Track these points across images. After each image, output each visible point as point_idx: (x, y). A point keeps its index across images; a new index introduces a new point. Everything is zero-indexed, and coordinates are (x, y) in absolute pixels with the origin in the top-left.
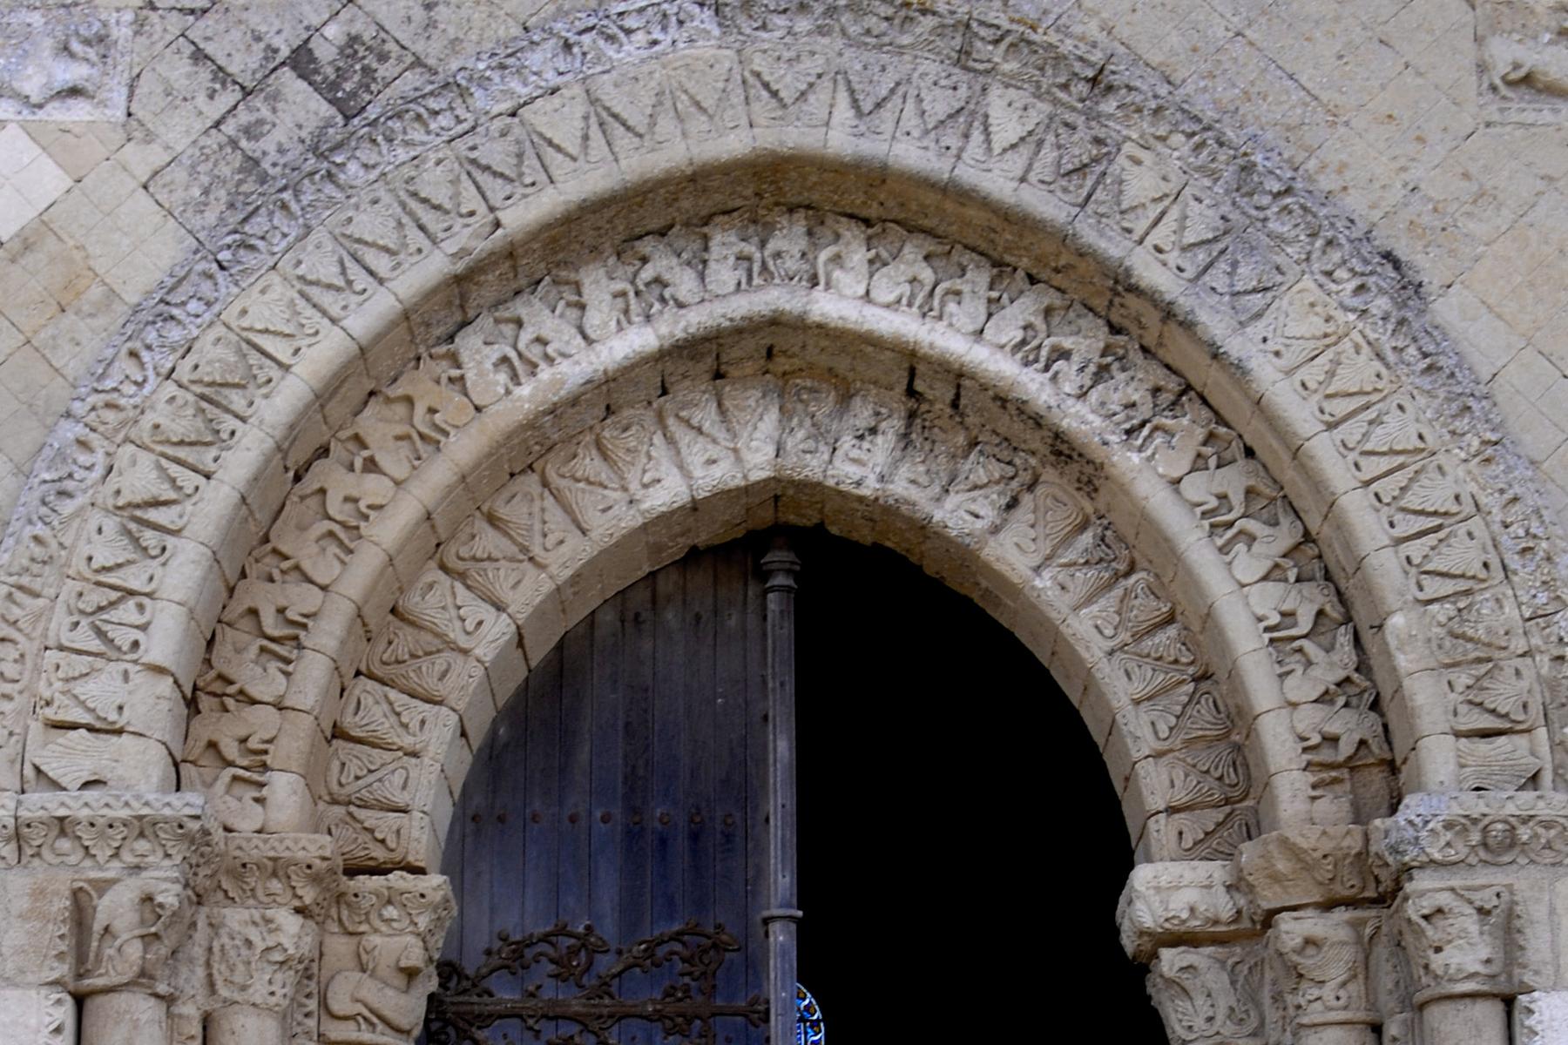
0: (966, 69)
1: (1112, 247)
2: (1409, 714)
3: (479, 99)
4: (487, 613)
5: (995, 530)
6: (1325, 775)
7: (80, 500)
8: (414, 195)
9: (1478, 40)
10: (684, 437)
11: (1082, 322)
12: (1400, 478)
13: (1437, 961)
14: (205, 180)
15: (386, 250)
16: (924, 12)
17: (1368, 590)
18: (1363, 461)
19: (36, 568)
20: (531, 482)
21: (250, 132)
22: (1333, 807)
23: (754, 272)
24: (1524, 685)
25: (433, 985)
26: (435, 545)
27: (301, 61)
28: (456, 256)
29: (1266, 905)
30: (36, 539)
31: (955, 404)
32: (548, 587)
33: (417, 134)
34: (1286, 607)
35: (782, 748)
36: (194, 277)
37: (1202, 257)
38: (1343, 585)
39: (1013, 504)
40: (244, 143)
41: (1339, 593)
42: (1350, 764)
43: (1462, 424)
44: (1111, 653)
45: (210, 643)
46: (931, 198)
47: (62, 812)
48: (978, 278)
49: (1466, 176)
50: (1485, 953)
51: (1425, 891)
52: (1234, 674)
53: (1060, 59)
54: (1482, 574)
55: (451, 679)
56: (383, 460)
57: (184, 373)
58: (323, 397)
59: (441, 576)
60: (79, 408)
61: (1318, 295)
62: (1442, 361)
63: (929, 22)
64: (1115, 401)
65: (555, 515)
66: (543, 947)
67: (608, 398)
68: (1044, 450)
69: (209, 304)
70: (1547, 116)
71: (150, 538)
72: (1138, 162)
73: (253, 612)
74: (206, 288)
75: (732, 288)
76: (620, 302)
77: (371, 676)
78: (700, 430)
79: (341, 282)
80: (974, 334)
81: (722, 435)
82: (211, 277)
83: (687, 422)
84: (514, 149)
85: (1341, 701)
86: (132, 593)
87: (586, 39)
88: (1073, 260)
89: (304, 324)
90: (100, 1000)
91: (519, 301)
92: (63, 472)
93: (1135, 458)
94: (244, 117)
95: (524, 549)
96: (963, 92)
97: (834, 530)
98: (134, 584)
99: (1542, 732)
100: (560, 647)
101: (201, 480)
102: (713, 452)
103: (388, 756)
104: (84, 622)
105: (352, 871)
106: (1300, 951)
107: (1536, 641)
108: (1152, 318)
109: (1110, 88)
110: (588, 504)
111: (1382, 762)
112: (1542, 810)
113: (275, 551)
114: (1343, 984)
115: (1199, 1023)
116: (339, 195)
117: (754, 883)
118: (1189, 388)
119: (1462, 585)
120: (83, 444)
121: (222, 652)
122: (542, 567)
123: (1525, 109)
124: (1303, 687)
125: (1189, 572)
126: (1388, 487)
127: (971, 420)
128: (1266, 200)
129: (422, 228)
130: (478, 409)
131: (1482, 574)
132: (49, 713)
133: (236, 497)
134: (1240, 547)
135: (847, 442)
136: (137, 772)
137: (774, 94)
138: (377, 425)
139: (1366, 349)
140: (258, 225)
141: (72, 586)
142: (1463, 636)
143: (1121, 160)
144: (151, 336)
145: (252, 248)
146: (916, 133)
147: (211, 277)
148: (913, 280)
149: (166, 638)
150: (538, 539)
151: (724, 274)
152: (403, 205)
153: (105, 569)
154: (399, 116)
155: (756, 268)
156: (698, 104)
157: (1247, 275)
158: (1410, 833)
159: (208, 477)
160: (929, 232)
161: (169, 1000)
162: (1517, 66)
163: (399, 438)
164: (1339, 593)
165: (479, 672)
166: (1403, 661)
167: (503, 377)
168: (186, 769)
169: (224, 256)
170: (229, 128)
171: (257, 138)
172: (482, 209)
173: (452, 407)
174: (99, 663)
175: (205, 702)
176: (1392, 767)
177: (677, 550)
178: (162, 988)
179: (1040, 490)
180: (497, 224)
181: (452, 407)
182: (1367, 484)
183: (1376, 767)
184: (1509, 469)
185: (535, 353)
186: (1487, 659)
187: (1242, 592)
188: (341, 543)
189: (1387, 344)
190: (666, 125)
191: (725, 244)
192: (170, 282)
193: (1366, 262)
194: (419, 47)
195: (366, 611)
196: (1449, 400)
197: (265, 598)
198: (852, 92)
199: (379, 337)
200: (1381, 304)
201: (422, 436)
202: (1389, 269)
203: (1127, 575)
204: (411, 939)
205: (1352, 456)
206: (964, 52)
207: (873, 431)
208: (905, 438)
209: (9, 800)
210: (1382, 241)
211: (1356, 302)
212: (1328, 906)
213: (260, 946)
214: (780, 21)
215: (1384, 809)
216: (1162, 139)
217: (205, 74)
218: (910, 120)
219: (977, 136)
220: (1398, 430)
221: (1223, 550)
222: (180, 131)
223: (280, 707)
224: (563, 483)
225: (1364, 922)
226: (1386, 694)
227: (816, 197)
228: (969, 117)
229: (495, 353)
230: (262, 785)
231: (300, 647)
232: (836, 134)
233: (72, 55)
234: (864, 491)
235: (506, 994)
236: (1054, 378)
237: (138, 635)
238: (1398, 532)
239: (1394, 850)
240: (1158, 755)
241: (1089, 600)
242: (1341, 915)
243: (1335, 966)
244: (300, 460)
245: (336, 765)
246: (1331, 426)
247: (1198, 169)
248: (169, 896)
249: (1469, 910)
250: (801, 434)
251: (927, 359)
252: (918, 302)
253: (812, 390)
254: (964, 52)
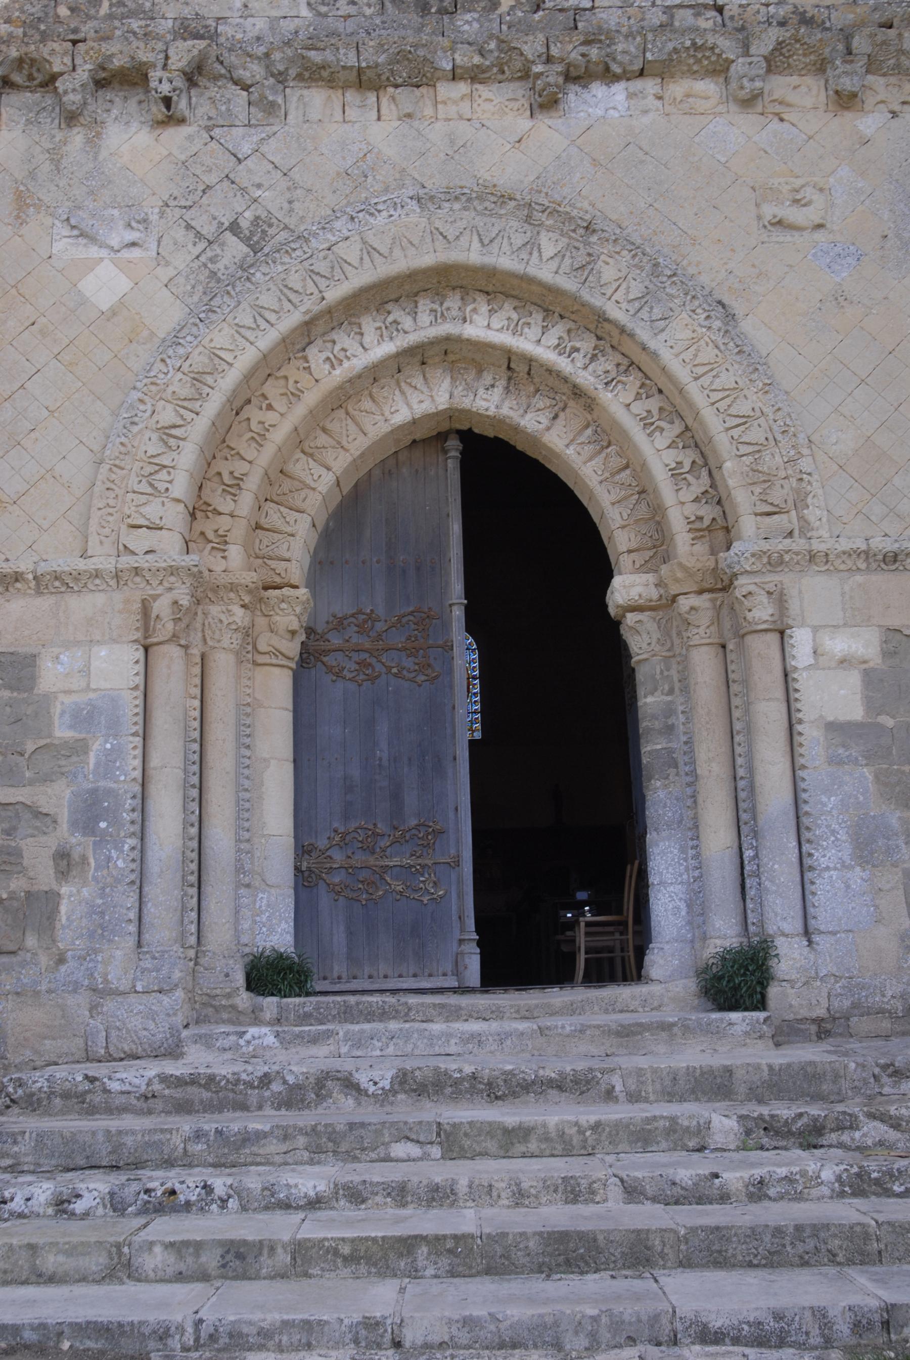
0: (530, 224)
1: (597, 301)
3: (314, 243)
4: (323, 471)
6: (698, 534)
7: (141, 426)
8: (286, 286)
9: (757, 205)
10: (409, 391)
11: (584, 335)
12: (728, 401)
14: (193, 282)
15: (274, 311)
16: (510, 199)
17: (715, 451)
18: (711, 394)
19: (122, 457)
20: (341, 413)
21: (213, 260)
22: (701, 548)
23: (438, 317)
24: (785, 491)
25: (303, 637)
26: (300, 442)
27: (234, 228)
30: (122, 444)
31: (529, 374)
32: (350, 459)
33: (286, 259)
34: (678, 460)
35: (456, 528)
36: (189, 325)
37: (637, 305)
38: (703, 449)
39: (556, 417)
40: (209, 265)
41: (702, 453)
42: (709, 529)
43: (754, 376)
44: (601, 482)
45: (200, 488)
47: (136, 565)
48: (538, 316)
49: (753, 266)
51: (744, 584)
52: (656, 490)
53: (571, 219)
54: (765, 443)
55: (308, 501)
56: (274, 404)
57: (185, 368)
58: (248, 378)
59: (302, 455)
60: (139, 385)
63: (513, 204)
64: (600, 370)
65: (352, 427)
66: (352, 620)
67: (374, 374)
69: (196, 337)
70: (789, 238)
71: (172, 442)
72: (607, 264)
73: (219, 474)
74: (194, 330)
75: (428, 324)
76: (379, 332)
77: (272, 501)
78: (415, 388)
79: (254, 326)
80: (537, 342)
81: (425, 390)
82: (196, 325)
84: (330, 265)
85: (704, 501)
86: (165, 467)
89: (237, 346)
90: (155, 648)
91: (334, 332)
92: (133, 414)
93: (609, 395)
94: (209, 253)
95: (339, 443)
96: (529, 234)
97: (476, 431)
98: (166, 463)
100: (356, 486)
102: (422, 397)
103: (281, 536)
104: (144, 480)
107: (790, 472)
108: (615, 333)
109: (594, 231)
110: (367, 422)
111: (723, 527)
113: (228, 446)
114: (708, 627)
116: (253, 287)
118: (633, 363)
119: (757, 448)
120: (141, 401)
121: (206, 492)
122: (347, 450)
123: (779, 236)
124: (687, 495)
125: (635, 445)
126: (722, 405)
127: (536, 380)
128: (665, 279)
129: (290, 301)
130: (317, 381)
131: (765, 443)
132: (130, 521)
133: (210, 423)
134: (657, 434)
135: (481, 391)
136: (169, 546)
137: (445, 237)
138: (272, 389)
139: (711, 344)
140: (216, 302)
141: (138, 465)
143: (600, 263)
144: (170, 352)
145: (214, 312)
147: (196, 325)
149: (181, 486)
150: (345, 438)
151: (425, 318)
152: (281, 291)
153: (153, 456)
154: (278, 251)
155: (439, 315)
156: (411, 243)
157: (657, 313)
158: (736, 559)
159: (197, 414)
161: (186, 647)
162: (775, 217)
163: (282, 395)
164: (702, 453)
165: (320, 498)
166: (731, 482)
167: (327, 366)
168: (191, 544)
169: (202, 316)
170: (203, 259)
171: (215, 263)
172: (316, 292)
173: (305, 380)
174: (151, 498)
175: (199, 514)
176: (727, 530)
177: (407, 441)
178: (183, 642)
179: (567, 410)
180: (323, 299)
181: (305, 380)
182: (713, 404)
183: (720, 530)
185: (341, 355)
186: (768, 481)
187: (658, 454)
188: (257, 442)
190: (397, 252)
191: (425, 305)
192: (178, 328)
193: (710, 305)
194: (286, 221)
195: (269, 472)
196: (748, 366)
197: (224, 468)
198: (479, 235)
199: (272, 350)
200: (717, 324)
201: (292, 394)
202: (720, 309)
203: (607, 447)
204: (293, 618)
205: (706, 392)
206: (529, 217)
207: (493, 386)
208: (507, 389)
210: (717, 296)
211: (706, 323)
213: (226, 622)
214: (447, 205)
215: (724, 548)
217: (191, 235)
218: (506, 247)
219: (536, 253)
220: (726, 380)
221: (649, 435)
222: (181, 261)
224: (355, 413)
226: (724, 497)
228: (532, 245)
229: (324, 356)
230: (225, 551)
231: (240, 489)
232: (473, 254)
233: (132, 228)
234: (490, 413)
236: (573, 360)
237: (168, 485)
238: (727, 425)
240: (623, 527)
241: (591, 459)
243: (704, 619)
244: (238, 406)
245: (257, 541)
246: (696, 379)
247: (635, 266)
248: (185, 601)
249: (763, 592)
250: (460, 388)
251: (516, 354)
252: (511, 327)
253: (465, 369)
254: (529, 217)
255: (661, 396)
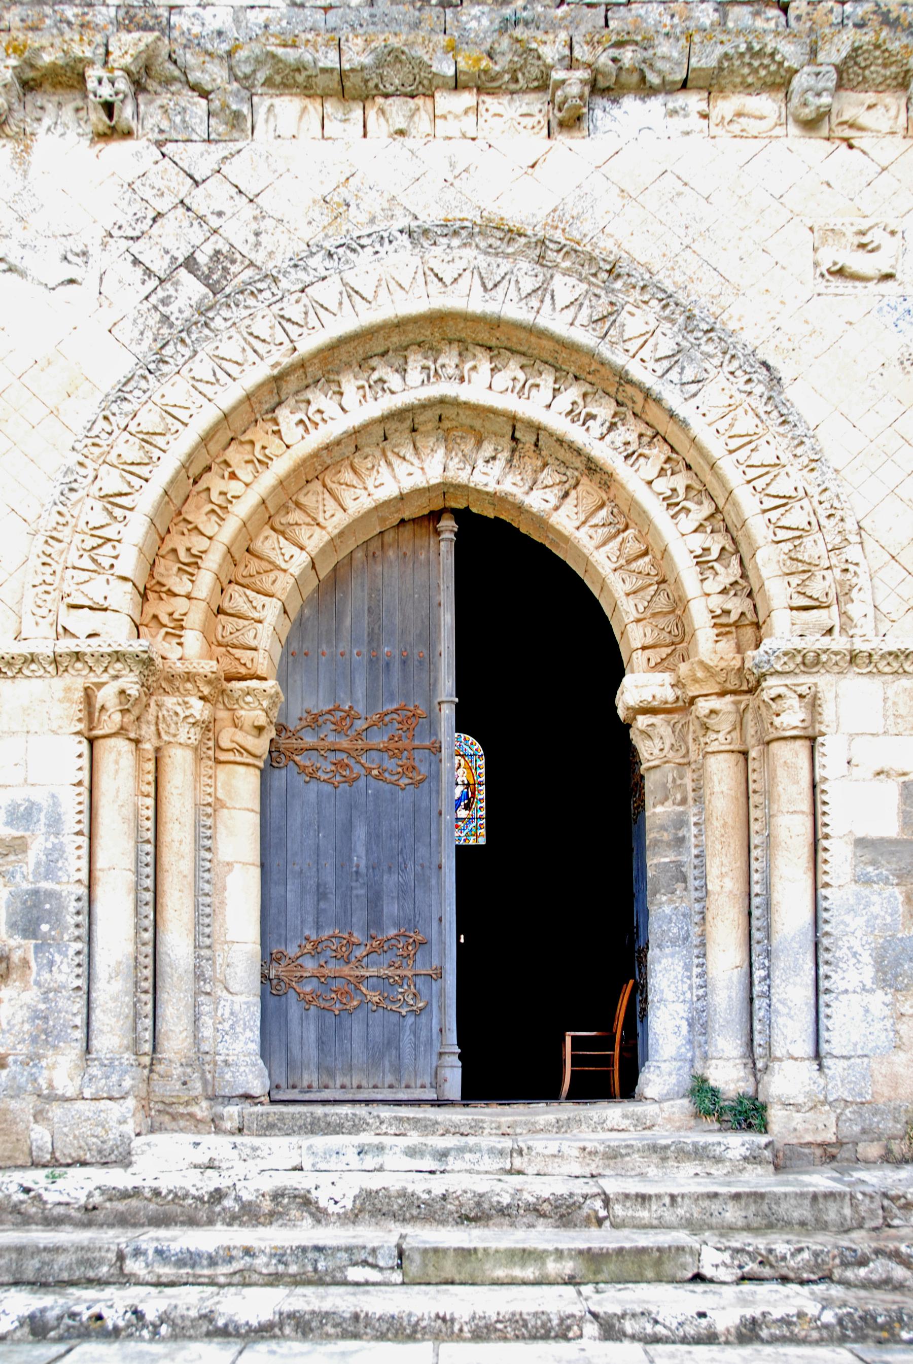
1: (619, 359)
2: (767, 600)
3: (284, 284)
5: (556, 508)
6: (724, 630)
8: (251, 334)
12: (766, 479)
13: (777, 721)
16: (520, 235)
17: (748, 536)
18: (748, 470)
22: (727, 646)
28: (274, 366)
29: (691, 694)
32: (327, 538)
33: (251, 301)
35: (447, 619)
39: (566, 495)
42: (736, 625)
43: (799, 451)
46: (523, 335)
50: (803, 717)
55: (278, 584)
57: (133, 428)
61: (727, 385)
62: (791, 418)
63: (523, 240)
68: (582, 467)
71: (118, 512)
72: (632, 315)
76: (361, 392)
77: (237, 583)
79: (213, 380)
81: (416, 461)
83: (398, 455)
86: (109, 540)
87: (341, 251)
88: (599, 367)
96: (541, 278)
99: (835, 608)
101: (142, 482)
103: (246, 623)
104: (86, 554)
105: (229, 679)
106: (708, 716)
107: (834, 561)
108: (639, 398)
109: (619, 276)
110: (347, 496)
111: (752, 623)
112: (835, 647)
115: (656, 751)
116: (211, 335)
117: (432, 686)
121: (160, 569)
122: (323, 528)
124: (713, 586)
125: (656, 528)
134: (682, 515)
137: (441, 280)
138: (235, 455)
141: (78, 538)
142: (797, 560)
143: (624, 314)
144: (114, 408)
145: (166, 362)
146: (516, 299)
148: (514, 379)
153: (95, 528)
154: (242, 292)
157: (689, 375)
160: (524, 354)
165: (292, 580)
166: (764, 573)
169: (152, 366)
175: (151, 595)
176: (757, 626)
179: (579, 488)
182: (749, 482)
183: (750, 626)
184: (823, 474)
185: (317, 418)
186: (808, 571)
187: (682, 538)
189: (761, 410)
195: (233, 550)
198: (482, 278)
203: (624, 531)
205: (743, 468)
206: (541, 257)
207: (494, 458)
208: (510, 461)
209: (50, 643)
210: (761, 356)
211: (748, 388)
212: (722, 694)
214: (444, 241)
216: (646, 303)
220: (766, 455)
223: (188, 597)
224: (334, 486)
225: (740, 702)
227: (463, 335)
228: (542, 291)
235: (310, 740)
237: (113, 561)
238: (765, 507)
239: (757, 666)
240: (638, 621)
241: (604, 544)
242: (729, 698)
244: (195, 473)
245: (220, 628)
250: (456, 460)
251: (522, 421)
255: (690, 473)
